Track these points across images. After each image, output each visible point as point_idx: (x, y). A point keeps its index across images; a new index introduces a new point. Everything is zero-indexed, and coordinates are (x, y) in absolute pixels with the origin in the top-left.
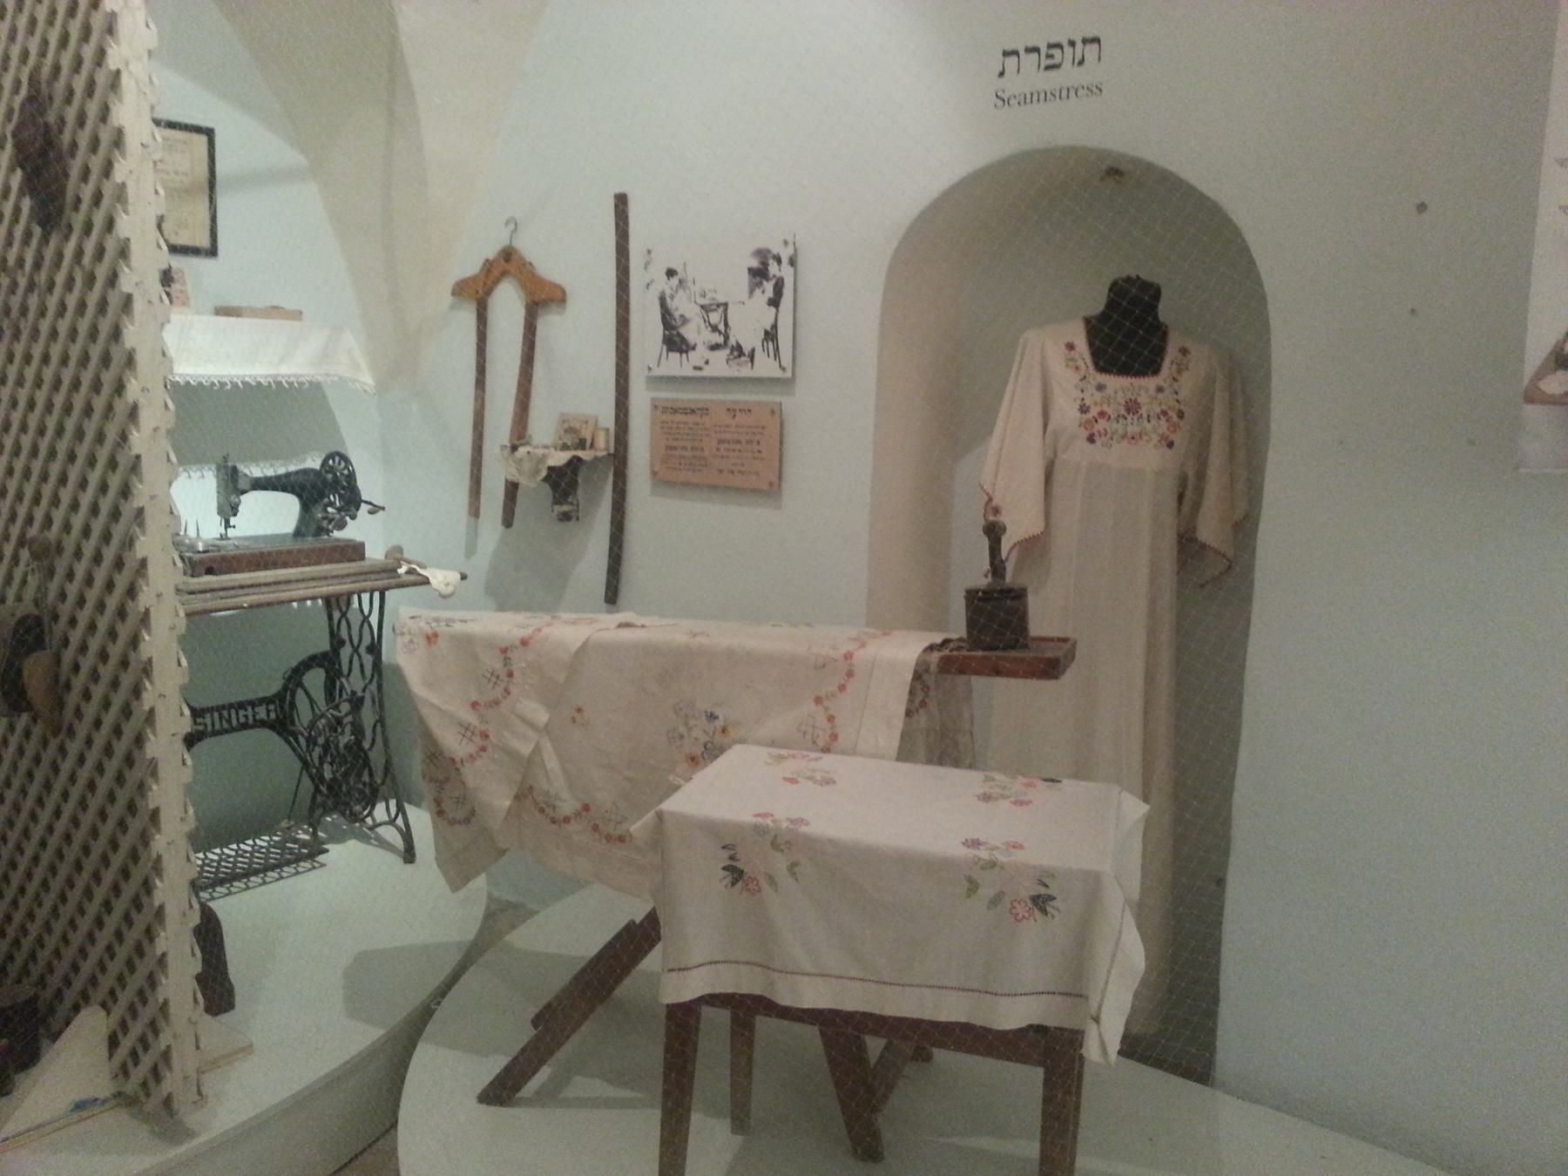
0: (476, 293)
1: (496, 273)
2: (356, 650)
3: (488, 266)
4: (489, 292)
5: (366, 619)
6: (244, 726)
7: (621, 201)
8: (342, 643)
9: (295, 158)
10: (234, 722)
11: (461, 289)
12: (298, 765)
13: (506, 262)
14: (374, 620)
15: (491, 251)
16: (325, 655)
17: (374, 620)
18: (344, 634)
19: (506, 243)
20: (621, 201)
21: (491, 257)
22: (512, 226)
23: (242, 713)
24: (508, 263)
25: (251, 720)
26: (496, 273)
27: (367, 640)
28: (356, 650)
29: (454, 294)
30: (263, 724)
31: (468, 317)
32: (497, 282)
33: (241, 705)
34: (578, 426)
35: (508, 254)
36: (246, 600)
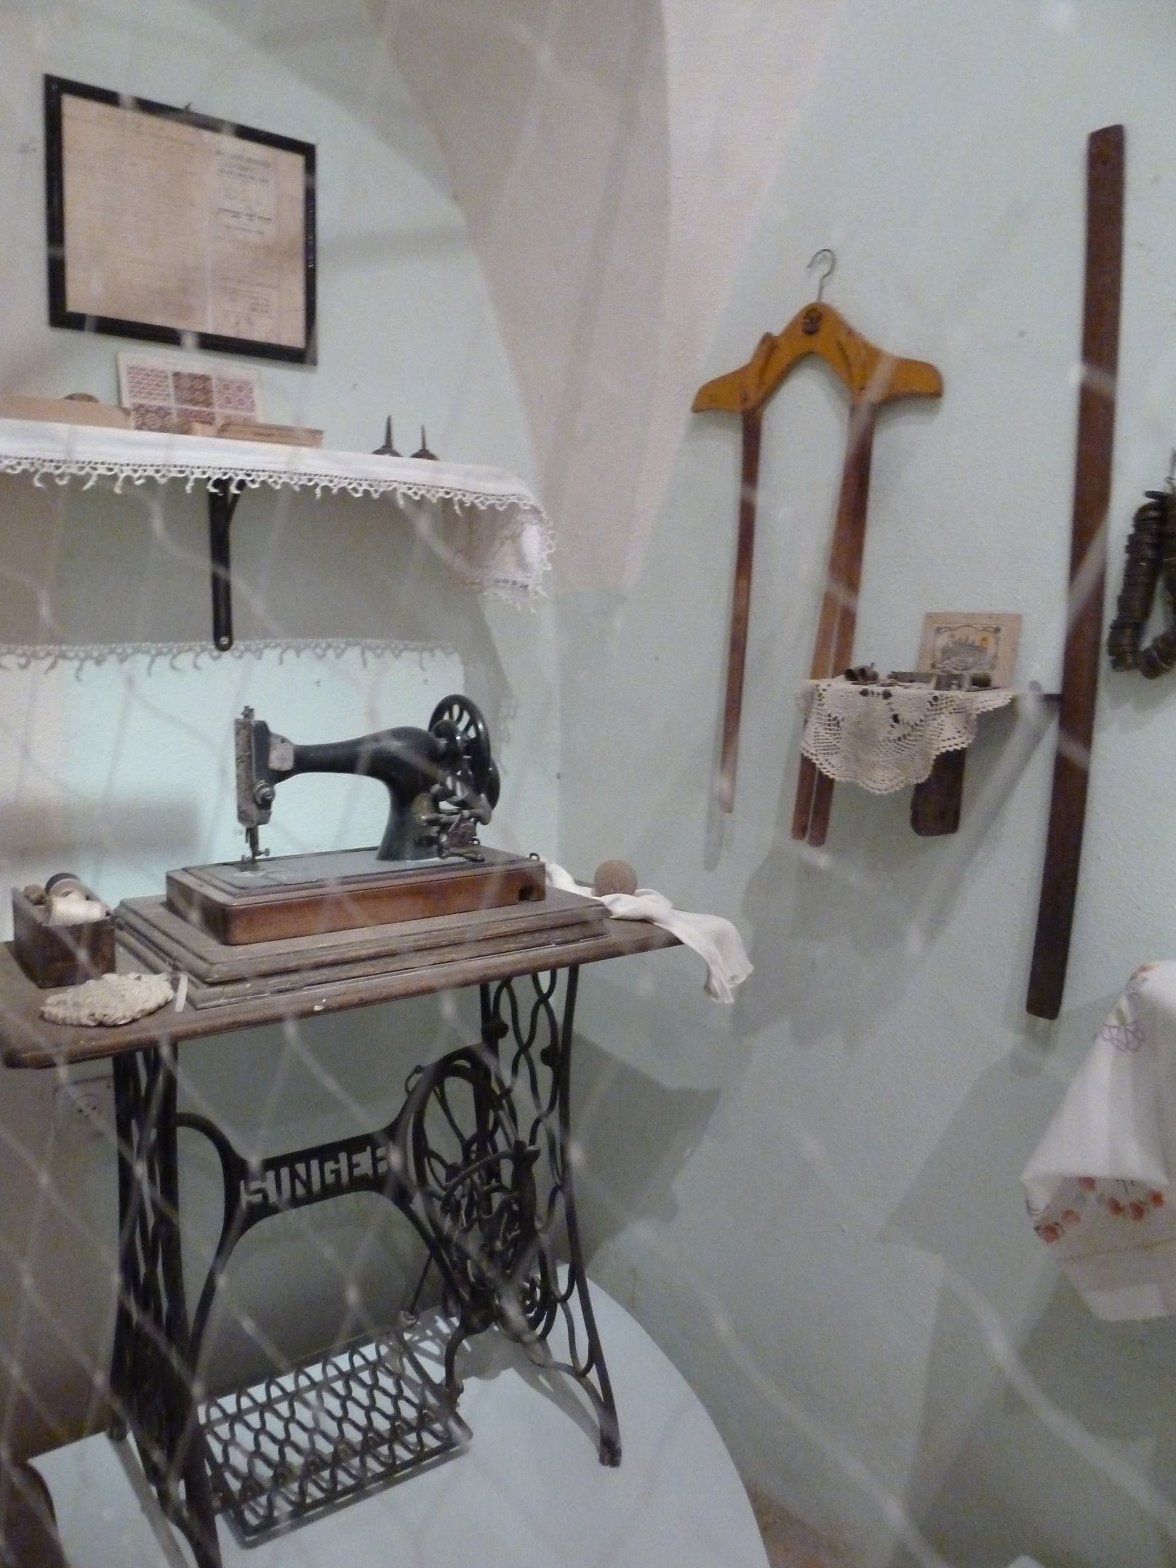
0: (741, 404)
1: (783, 357)
2: (524, 1049)
3: (769, 345)
4: (769, 392)
5: (543, 999)
6: (328, 1191)
7: (1106, 153)
8: (502, 1030)
9: (448, 214)
10: (316, 1186)
11: (710, 401)
12: (428, 1252)
13: (816, 335)
14: (557, 1001)
15: (778, 319)
16: (466, 1053)
17: (557, 1001)
18: (506, 1015)
19: (813, 300)
20: (1106, 153)
21: (777, 330)
22: (825, 268)
23: (329, 1166)
24: (816, 335)
25: (345, 1177)
26: (783, 357)
27: (543, 1040)
28: (524, 1049)
29: (697, 409)
30: (359, 1184)
31: (725, 447)
32: (782, 377)
33: (325, 1153)
34: (975, 638)
35: (814, 320)
36: (322, 995)
